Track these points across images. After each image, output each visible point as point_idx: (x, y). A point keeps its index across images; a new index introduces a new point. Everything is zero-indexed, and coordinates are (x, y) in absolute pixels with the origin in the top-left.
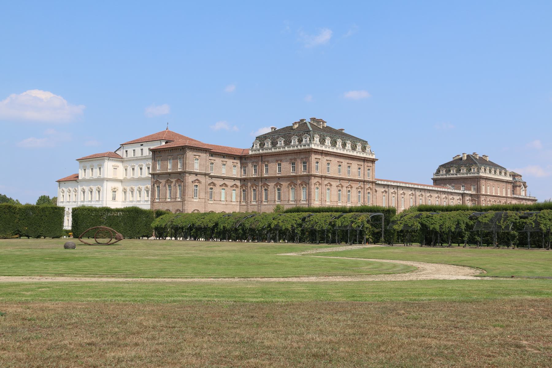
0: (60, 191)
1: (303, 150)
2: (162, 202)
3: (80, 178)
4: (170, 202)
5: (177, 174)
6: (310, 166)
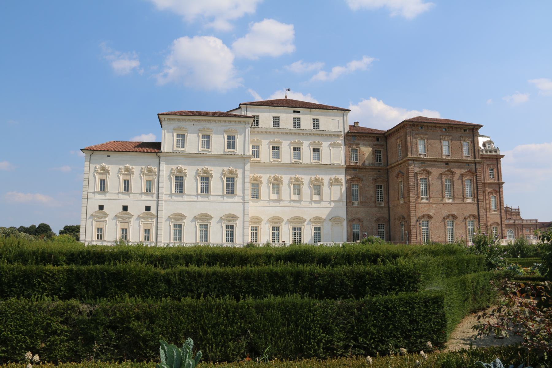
0: (92, 170)
1: (489, 155)
2: (435, 203)
3: (165, 148)
4: (452, 204)
5: (461, 164)
6: (499, 174)
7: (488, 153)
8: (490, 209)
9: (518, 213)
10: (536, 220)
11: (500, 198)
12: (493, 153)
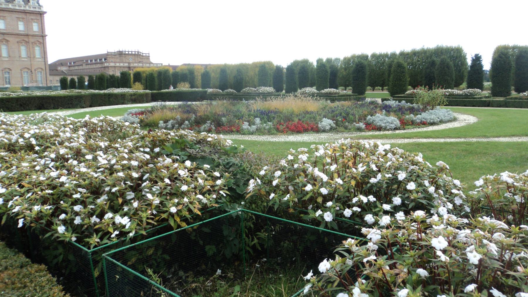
7: (32, 9)
8: (34, 57)
9: (148, 57)
10: (162, 64)
11: (44, 48)
12: (37, 10)
